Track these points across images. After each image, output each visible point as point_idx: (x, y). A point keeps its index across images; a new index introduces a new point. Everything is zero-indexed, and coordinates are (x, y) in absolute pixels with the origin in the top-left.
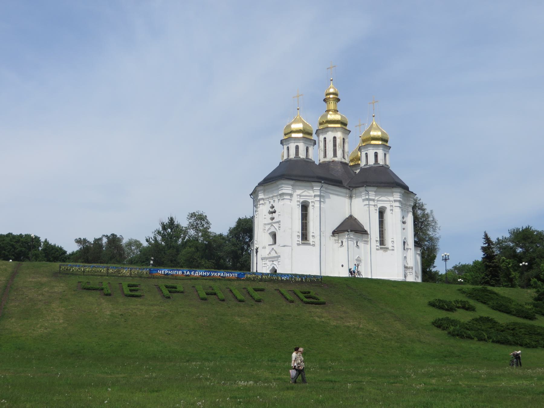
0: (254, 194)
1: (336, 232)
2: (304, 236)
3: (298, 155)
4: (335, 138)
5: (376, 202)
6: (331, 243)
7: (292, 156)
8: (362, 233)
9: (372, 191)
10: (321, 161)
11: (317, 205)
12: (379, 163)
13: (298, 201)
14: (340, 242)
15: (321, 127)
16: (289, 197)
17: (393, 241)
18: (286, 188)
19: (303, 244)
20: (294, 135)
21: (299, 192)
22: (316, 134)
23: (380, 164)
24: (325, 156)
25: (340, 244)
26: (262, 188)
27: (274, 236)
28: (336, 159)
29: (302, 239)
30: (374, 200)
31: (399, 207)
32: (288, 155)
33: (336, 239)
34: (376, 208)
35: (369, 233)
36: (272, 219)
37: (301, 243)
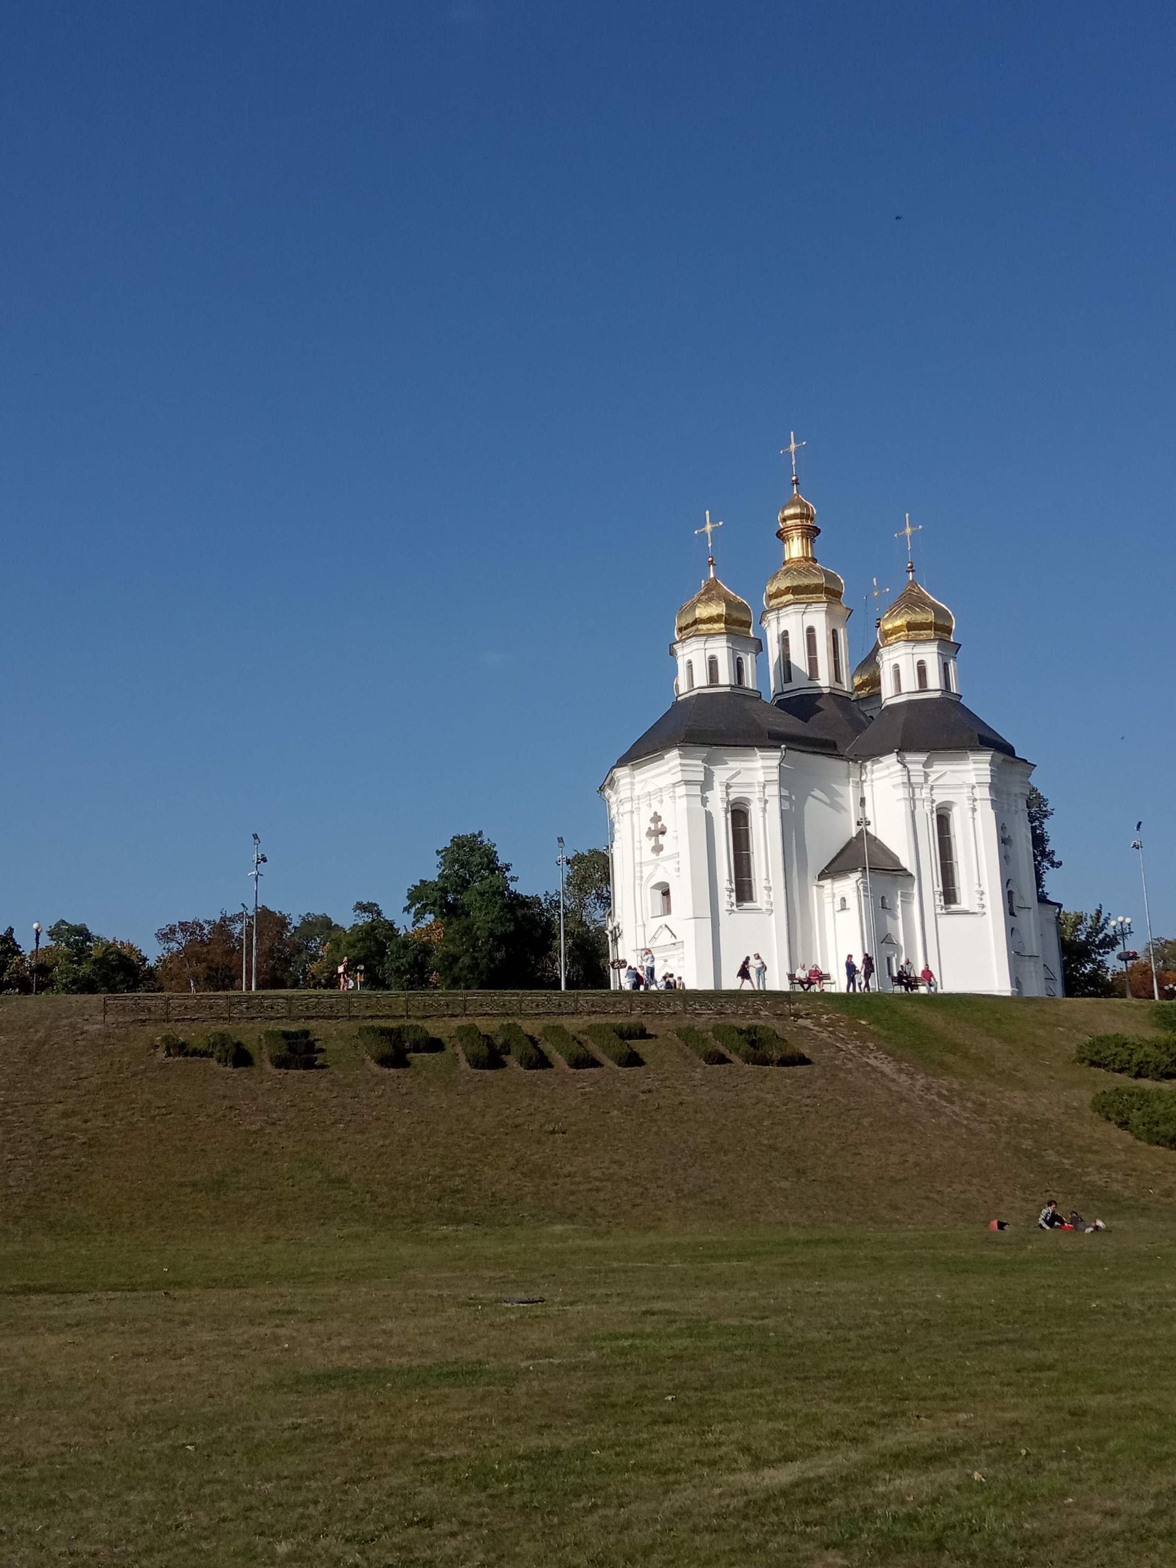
2: (743, 891)
3: (717, 681)
14: (838, 900)
25: (838, 907)
35: (914, 873)
36: (658, 849)
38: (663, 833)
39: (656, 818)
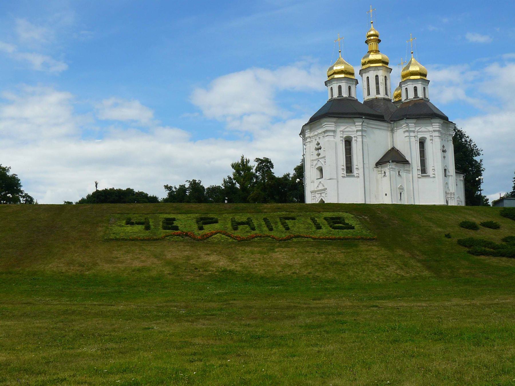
0: (302, 133)
2: (349, 169)
3: (341, 94)
4: (377, 76)
5: (416, 133)
6: (375, 174)
7: (336, 95)
8: (404, 164)
9: (411, 123)
10: (365, 99)
11: (360, 139)
12: (418, 96)
13: (341, 137)
14: (383, 172)
15: (364, 67)
16: (332, 134)
17: (434, 169)
18: (328, 125)
20: (336, 76)
21: (342, 128)
22: (359, 74)
23: (420, 97)
24: (369, 94)
25: (383, 175)
26: (308, 127)
27: (321, 170)
28: (379, 96)
29: (347, 172)
30: (414, 132)
31: (439, 136)
32: (332, 96)
33: (379, 170)
34: (416, 139)
35: (410, 163)
36: (319, 155)
37: (345, 176)
38: (320, 149)
39: (318, 144)
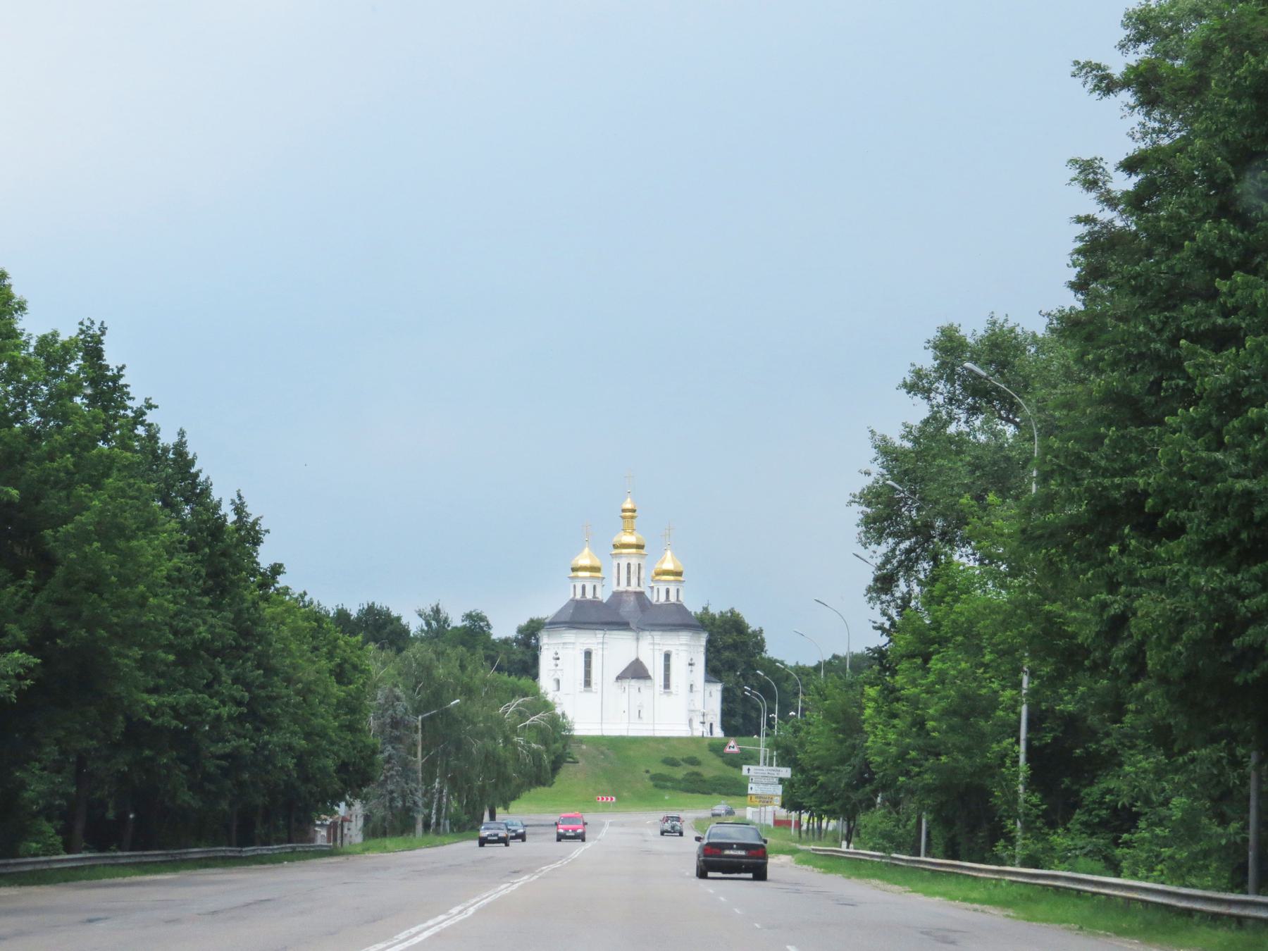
1: (619, 678)
2: (588, 683)
4: (629, 564)
6: (612, 688)
7: (578, 596)
19: (585, 691)
28: (630, 589)
30: (659, 644)
